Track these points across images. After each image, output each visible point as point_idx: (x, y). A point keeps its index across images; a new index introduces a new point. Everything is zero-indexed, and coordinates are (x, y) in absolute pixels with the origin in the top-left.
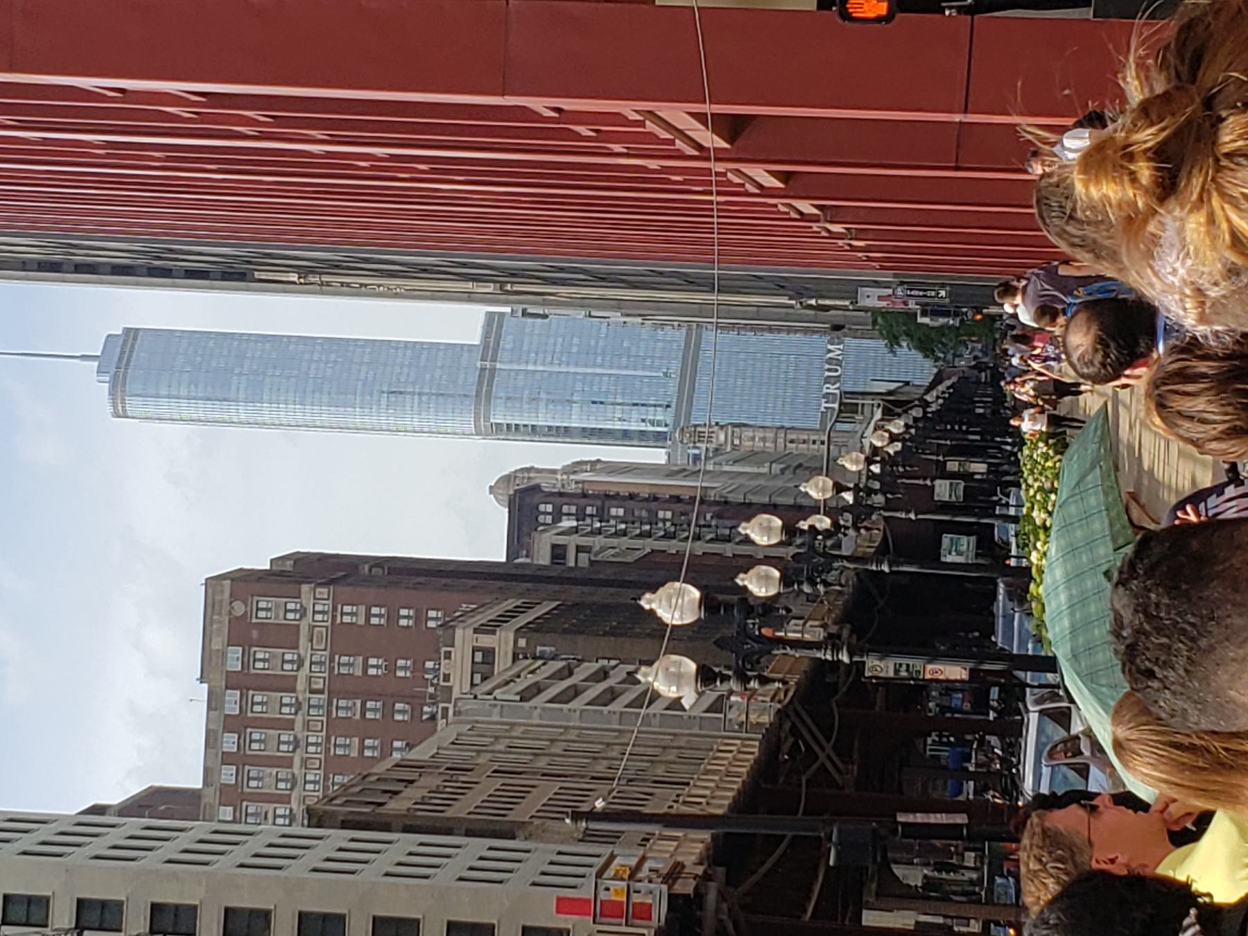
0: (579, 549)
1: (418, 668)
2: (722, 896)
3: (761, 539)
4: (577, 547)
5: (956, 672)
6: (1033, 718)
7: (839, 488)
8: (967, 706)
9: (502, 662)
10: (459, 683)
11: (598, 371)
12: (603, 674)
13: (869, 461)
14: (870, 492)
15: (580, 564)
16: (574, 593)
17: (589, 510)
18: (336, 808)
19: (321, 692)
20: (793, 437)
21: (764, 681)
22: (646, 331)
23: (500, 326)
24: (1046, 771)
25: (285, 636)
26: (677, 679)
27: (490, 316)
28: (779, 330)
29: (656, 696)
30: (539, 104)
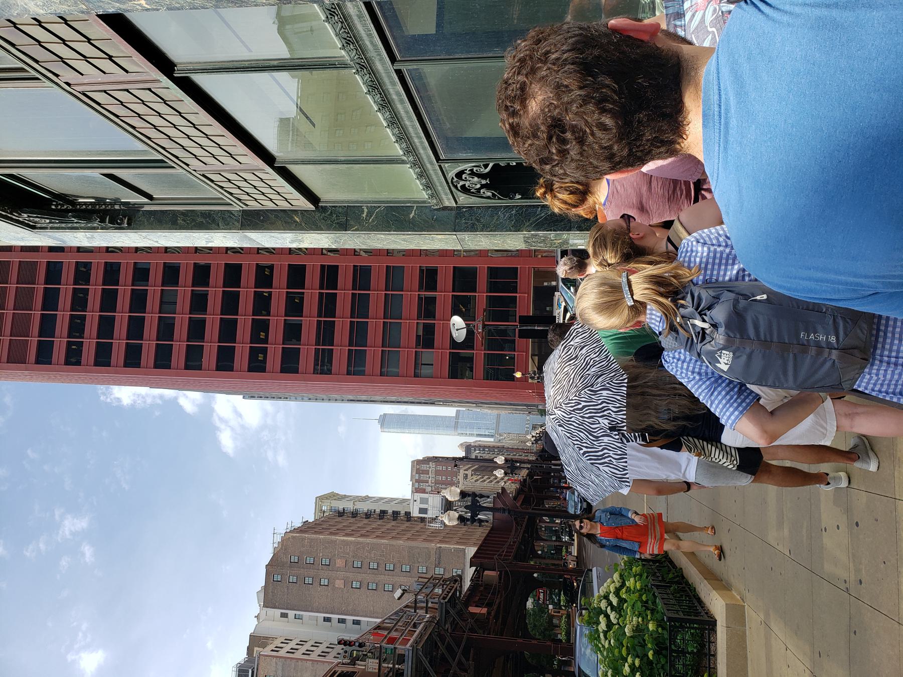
0: (481, 456)
9: (469, 476)
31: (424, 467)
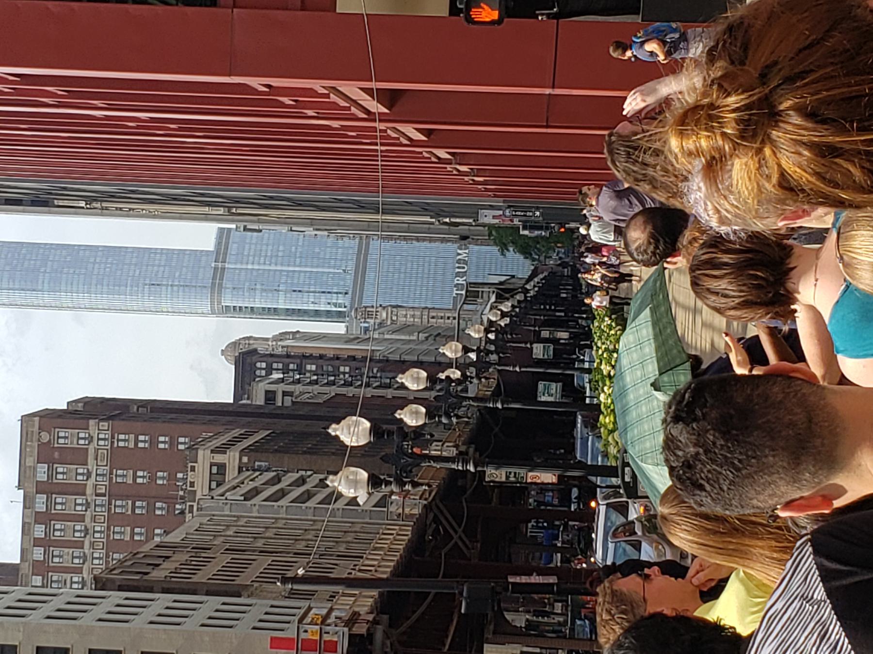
0: (285, 394)
1: (172, 477)
2: (386, 635)
3: (412, 386)
4: (283, 392)
5: (548, 477)
6: (603, 509)
7: (466, 350)
8: (556, 502)
9: (231, 473)
10: (201, 489)
11: (297, 269)
12: (302, 481)
13: (487, 331)
14: (489, 352)
15: (286, 404)
16: (282, 425)
17: (291, 366)
19: (104, 495)
20: (434, 314)
21: (415, 485)
22: (331, 240)
23: (228, 237)
24: (611, 546)
25: (78, 456)
26: (355, 484)
27: (221, 230)
28: (424, 239)
29: (340, 495)
30: (255, 82)
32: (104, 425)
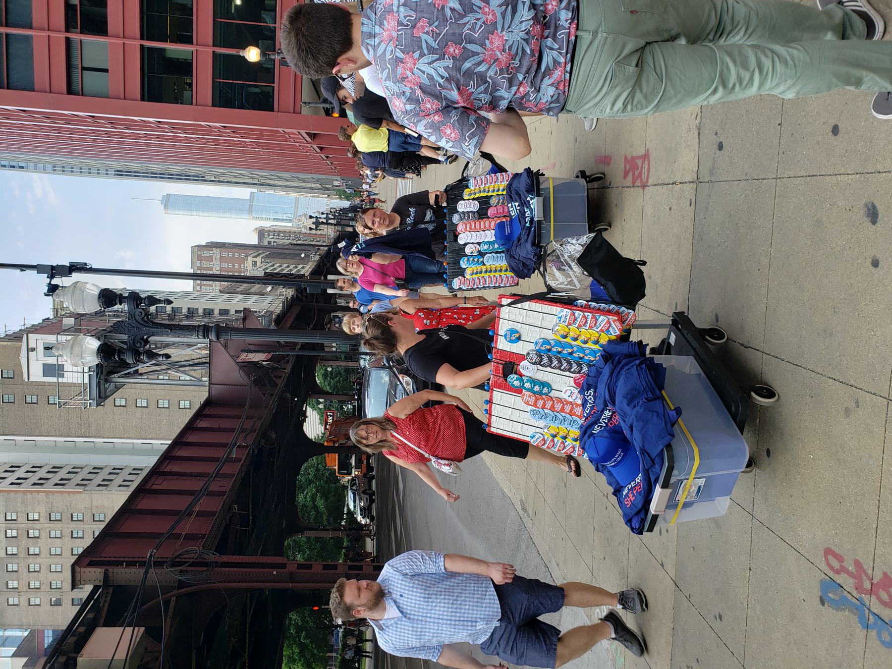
0: (274, 242)
1: (240, 266)
9: (259, 264)
12: (281, 266)
16: (274, 250)
18: (226, 290)
31: (206, 253)
32: (218, 249)
